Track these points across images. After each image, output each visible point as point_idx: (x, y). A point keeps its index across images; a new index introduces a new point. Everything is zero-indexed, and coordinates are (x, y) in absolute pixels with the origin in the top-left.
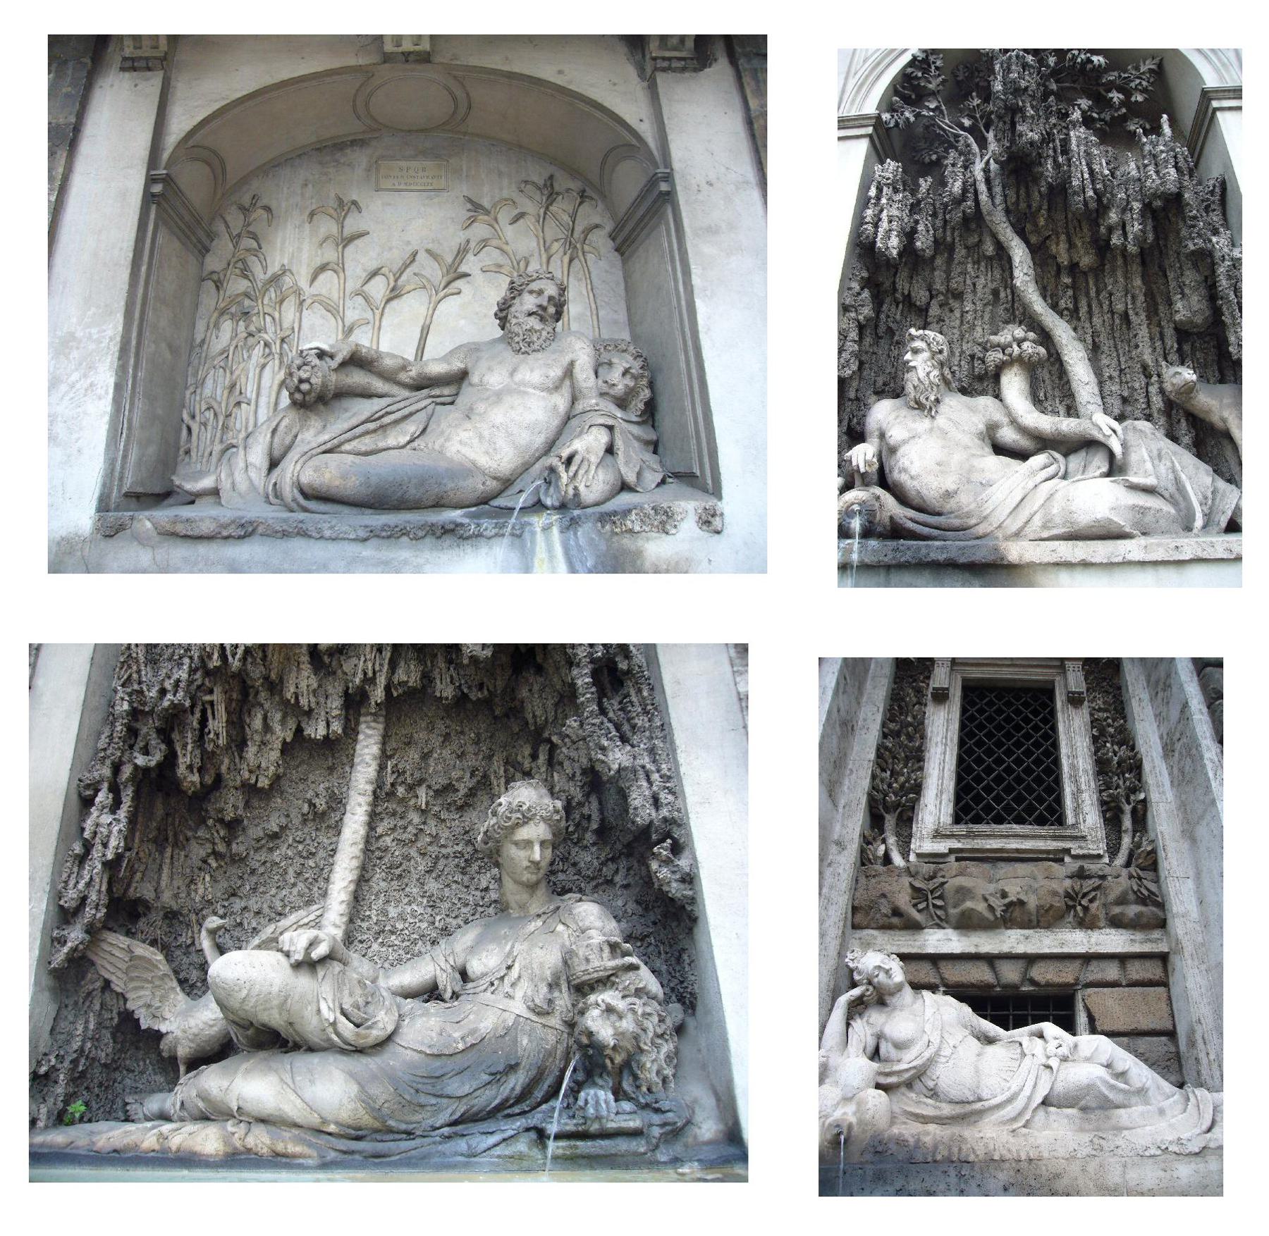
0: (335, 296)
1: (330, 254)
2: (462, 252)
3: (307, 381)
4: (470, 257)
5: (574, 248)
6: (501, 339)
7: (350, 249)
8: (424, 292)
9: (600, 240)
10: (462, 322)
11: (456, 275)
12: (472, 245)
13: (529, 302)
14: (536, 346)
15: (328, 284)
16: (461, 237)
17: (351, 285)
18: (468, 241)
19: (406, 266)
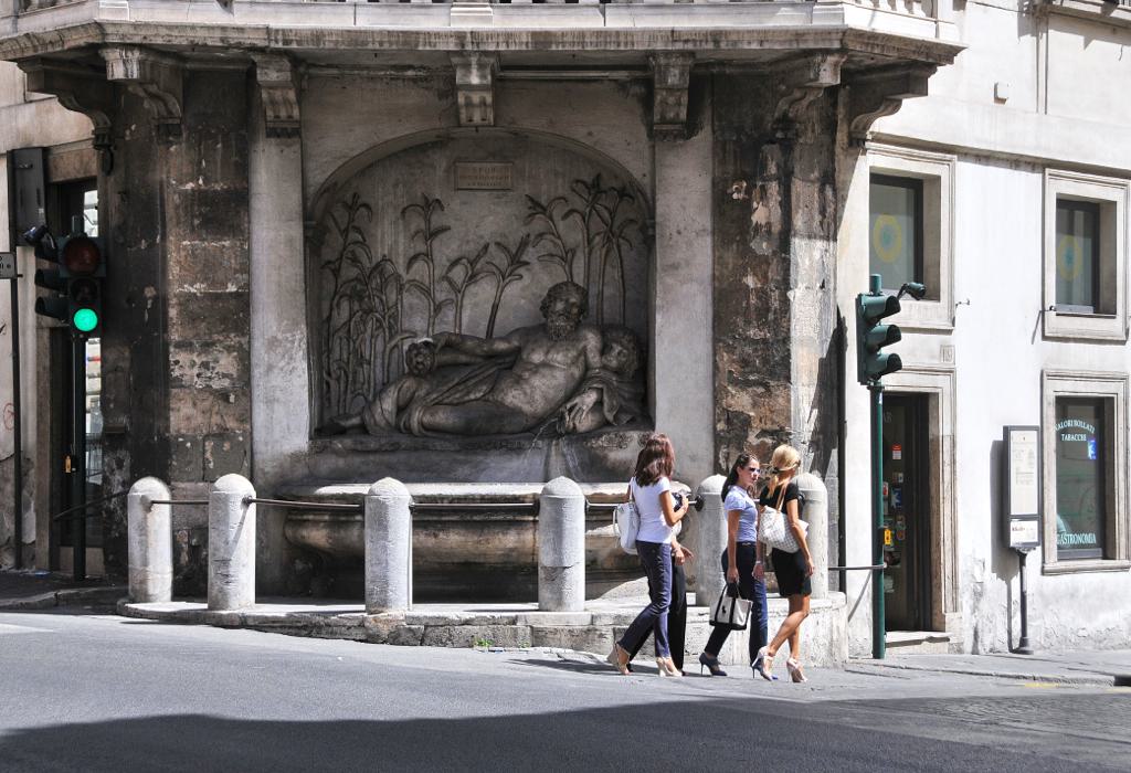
0: (427, 283)
2: (524, 244)
3: (422, 363)
4: (530, 249)
7: (436, 243)
9: (632, 232)
10: (523, 301)
11: (517, 261)
12: (532, 238)
13: (560, 306)
15: (420, 268)
16: (523, 231)
18: (528, 235)
19: (479, 257)
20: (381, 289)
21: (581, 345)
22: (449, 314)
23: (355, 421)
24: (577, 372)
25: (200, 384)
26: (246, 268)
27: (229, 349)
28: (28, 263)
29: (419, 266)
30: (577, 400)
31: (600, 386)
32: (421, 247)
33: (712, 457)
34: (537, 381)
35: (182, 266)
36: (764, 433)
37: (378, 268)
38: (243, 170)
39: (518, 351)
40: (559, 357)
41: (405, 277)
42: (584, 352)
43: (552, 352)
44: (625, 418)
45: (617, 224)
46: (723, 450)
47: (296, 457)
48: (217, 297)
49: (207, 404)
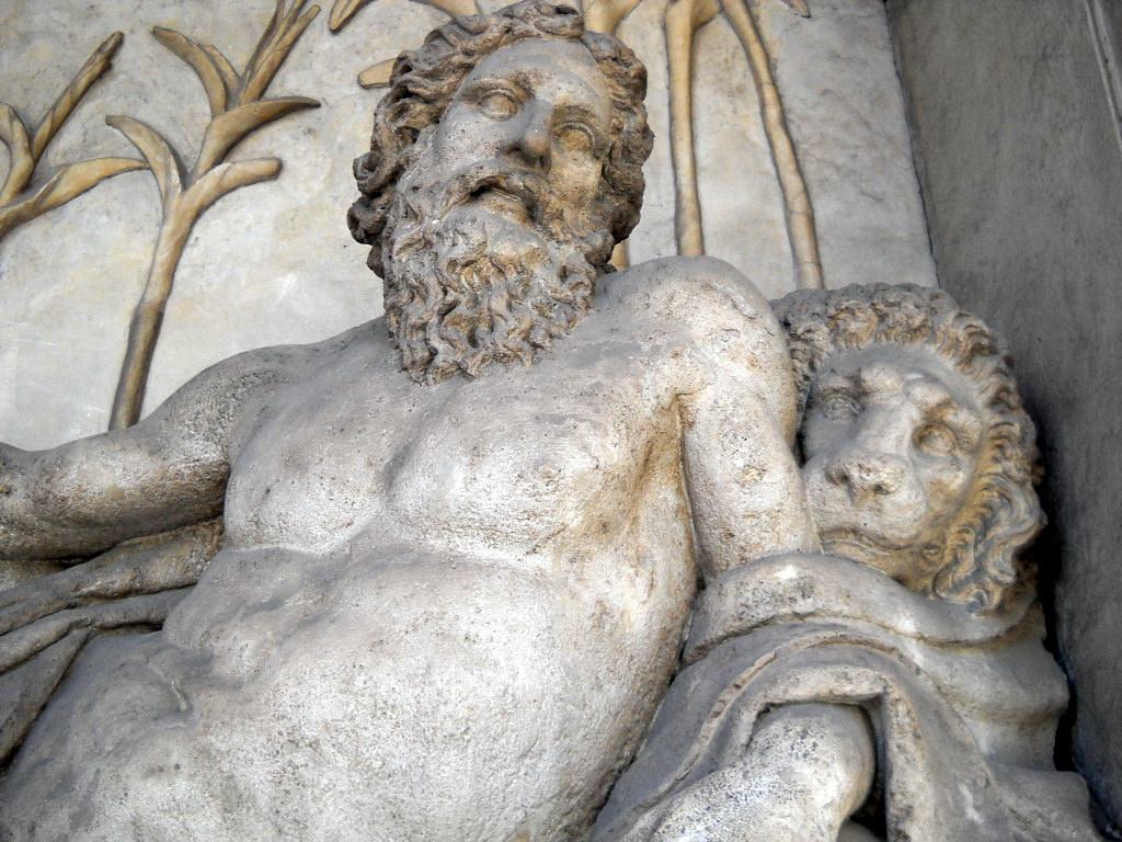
4: (318, 40)
6: (381, 333)
8: (144, 184)
10: (288, 283)
13: (471, 139)
14: (508, 333)
21: (662, 378)
24: (635, 596)
31: (862, 684)
39: (200, 510)
42: (671, 448)
43: (435, 447)
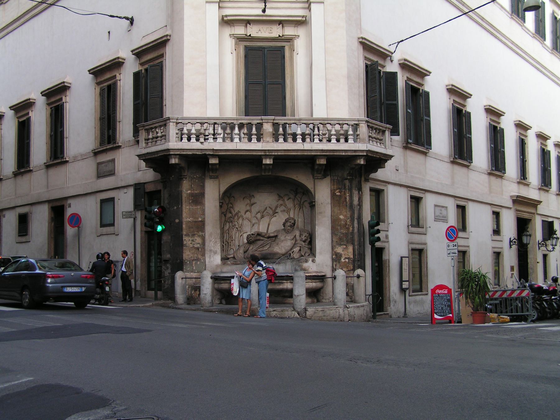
1: (248, 208)
2: (276, 207)
5: (301, 206)
6: (284, 230)
7: (253, 207)
9: (307, 204)
11: (275, 212)
16: (277, 203)
17: (253, 215)
20: (238, 219)
22: (256, 226)
23: (232, 256)
24: (293, 242)
25: (191, 246)
26: (204, 214)
27: (199, 236)
28: (139, 215)
29: (248, 213)
30: (294, 250)
32: (248, 208)
33: (331, 265)
34: (282, 244)
35: (187, 213)
36: (346, 258)
37: (237, 214)
38: (203, 187)
40: (289, 238)
41: (244, 216)
42: (295, 236)
44: (307, 254)
45: (302, 201)
46: (335, 263)
47: (217, 266)
48: (196, 222)
49: (193, 251)
